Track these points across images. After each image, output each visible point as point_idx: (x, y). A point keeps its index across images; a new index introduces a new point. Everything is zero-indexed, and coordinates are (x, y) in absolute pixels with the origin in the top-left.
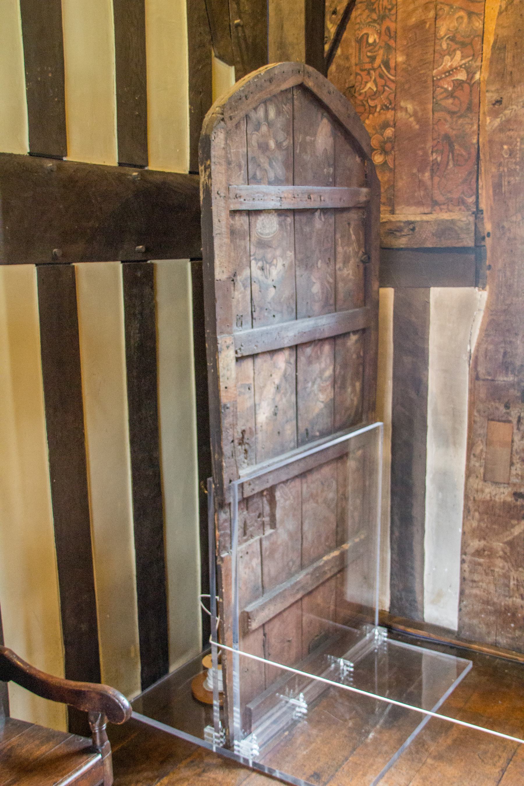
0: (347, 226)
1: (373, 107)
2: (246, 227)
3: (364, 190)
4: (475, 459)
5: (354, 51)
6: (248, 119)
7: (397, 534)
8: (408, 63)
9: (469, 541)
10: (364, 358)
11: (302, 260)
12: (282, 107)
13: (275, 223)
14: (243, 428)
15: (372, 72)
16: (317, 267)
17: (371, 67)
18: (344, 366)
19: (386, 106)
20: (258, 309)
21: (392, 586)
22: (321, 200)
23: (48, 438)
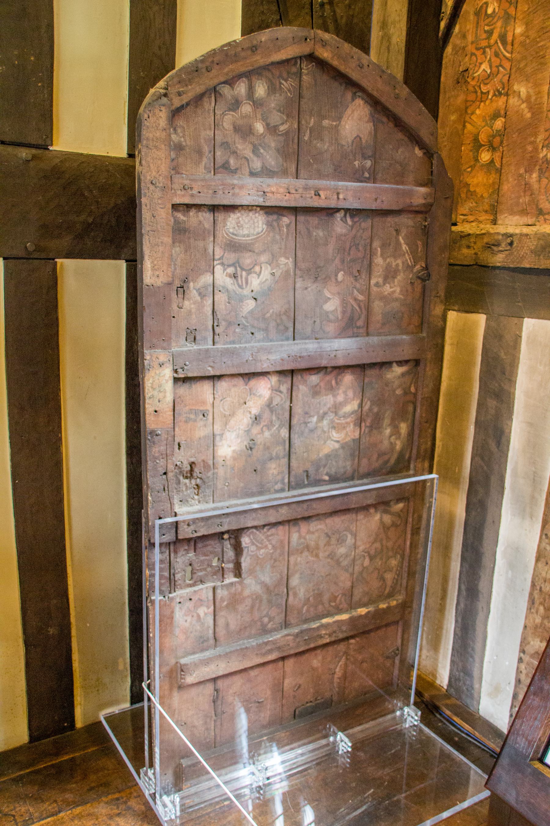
0: (394, 233)
1: (485, 93)
2: (208, 225)
3: (423, 190)
4: (547, 540)
5: (472, 26)
6: (218, 95)
7: (462, 605)
8: (526, 34)
9: (530, 639)
10: (415, 395)
11: (309, 270)
12: (280, 83)
13: (260, 223)
14: (192, 460)
15: (488, 50)
16: (336, 279)
17: (487, 44)
18: (380, 401)
19: (498, 91)
20: (223, 324)
21: (452, 662)
22: (338, 198)
23: (11, 438)
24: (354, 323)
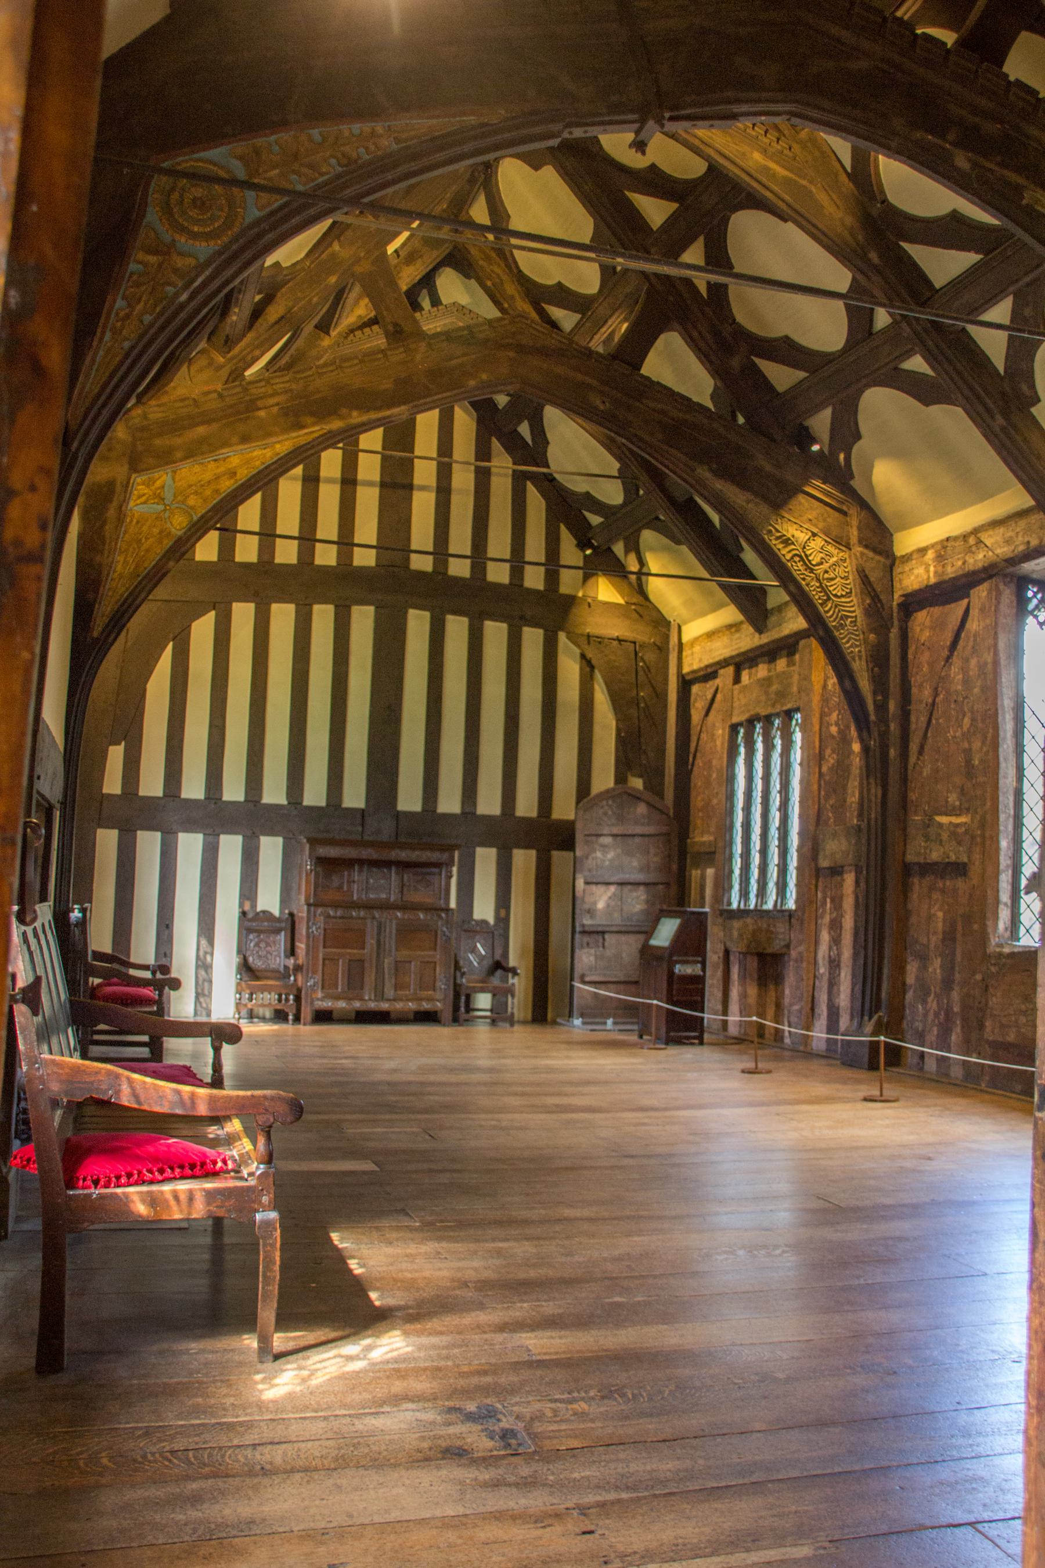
24: (641, 870)
